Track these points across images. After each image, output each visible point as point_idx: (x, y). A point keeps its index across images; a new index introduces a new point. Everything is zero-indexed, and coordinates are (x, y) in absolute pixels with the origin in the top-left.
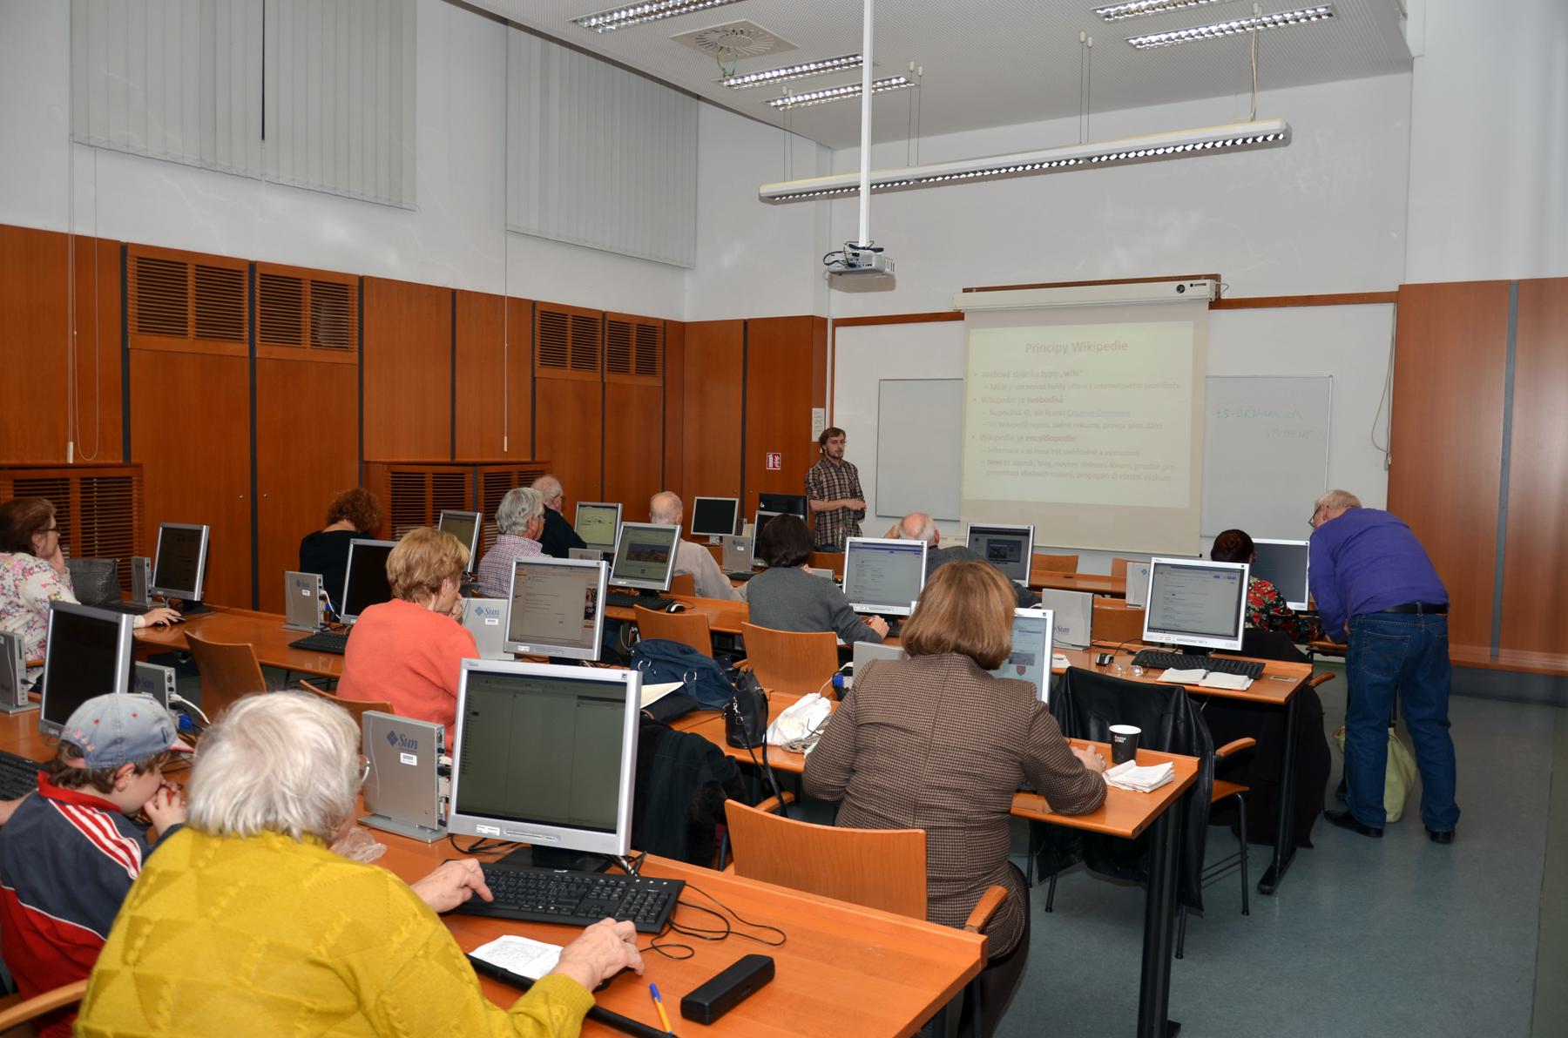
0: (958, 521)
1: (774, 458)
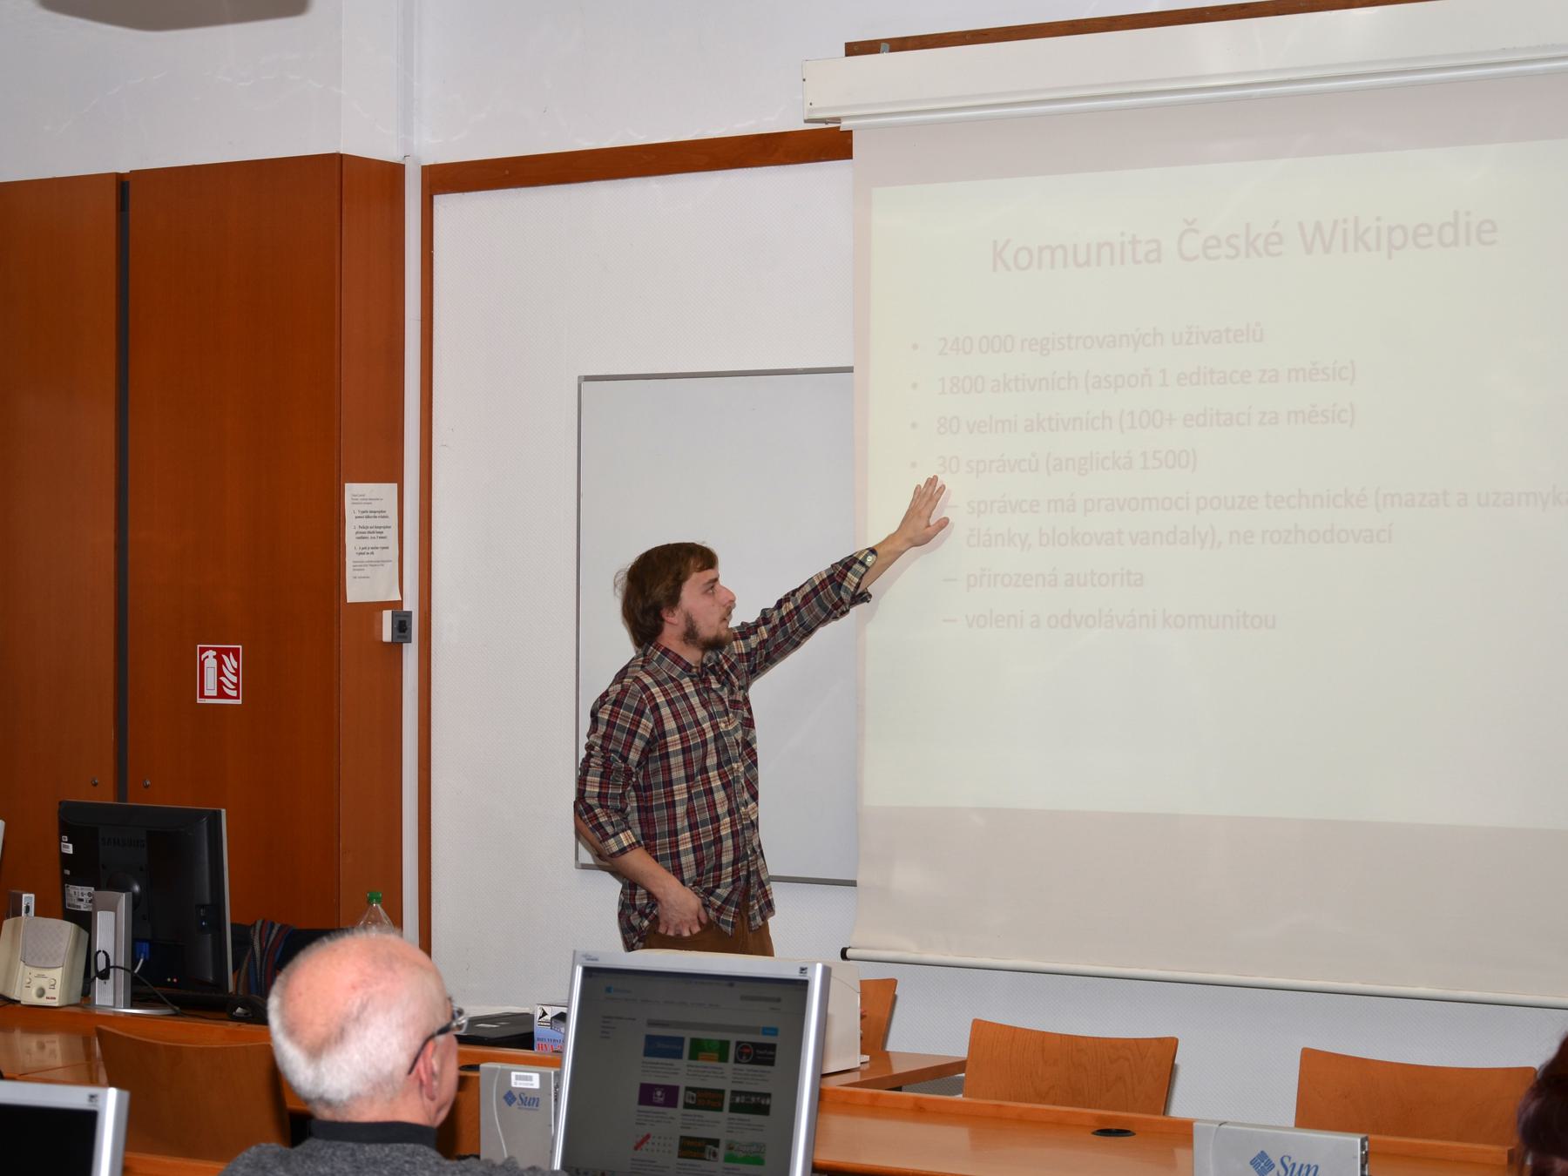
0: (853, 884)
1: (221, 663)
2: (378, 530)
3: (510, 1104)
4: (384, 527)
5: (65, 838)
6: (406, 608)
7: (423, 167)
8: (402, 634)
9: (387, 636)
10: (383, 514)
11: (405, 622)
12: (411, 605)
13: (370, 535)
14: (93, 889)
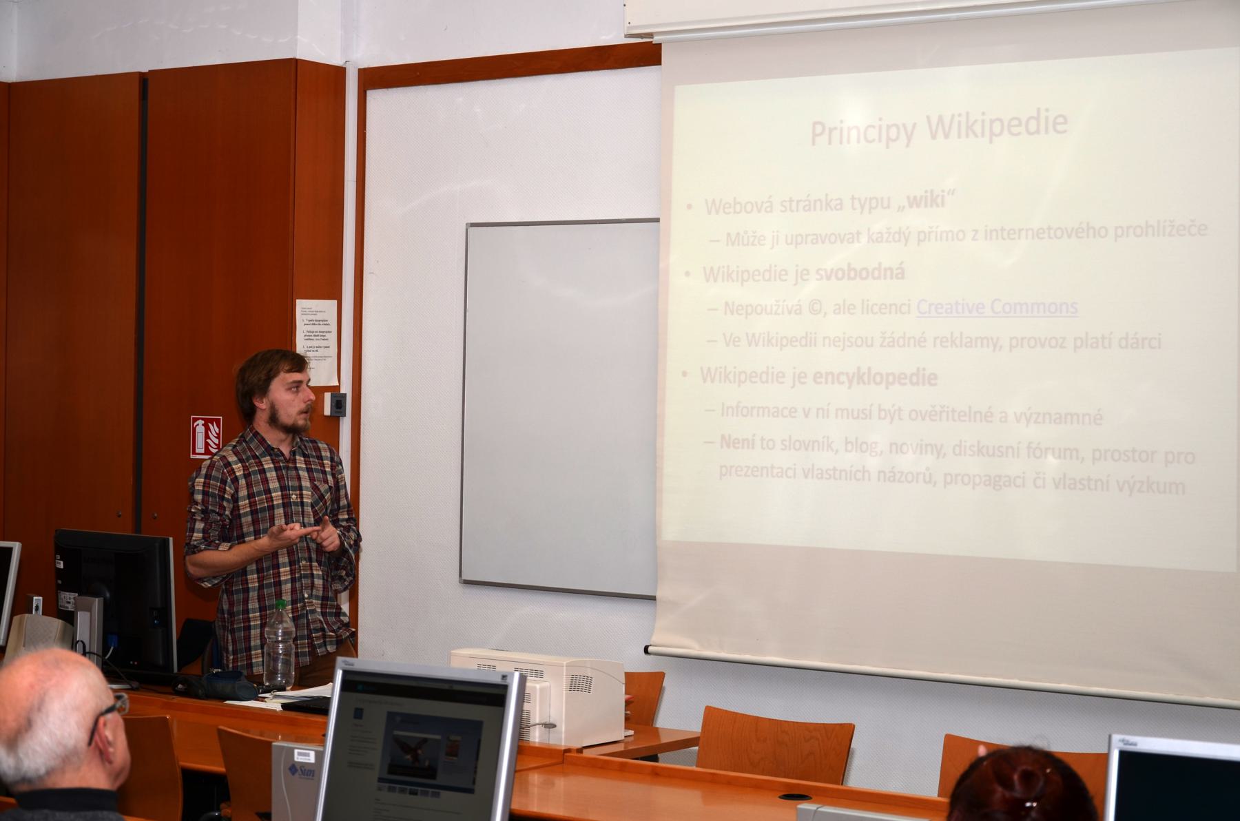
0: (653, 598)
1: (207, 429)
2: (321, 334)
3: (293, 774)
4: (327, 332)
5: (58, 557)
6: (342, 391)
7: (359, 69)
8: (339, 410)
9: (327, 411)
10: (325, 323)
11: (340, 401)
12: (346, 389)
13: (315, 338)
14: (77, 594)
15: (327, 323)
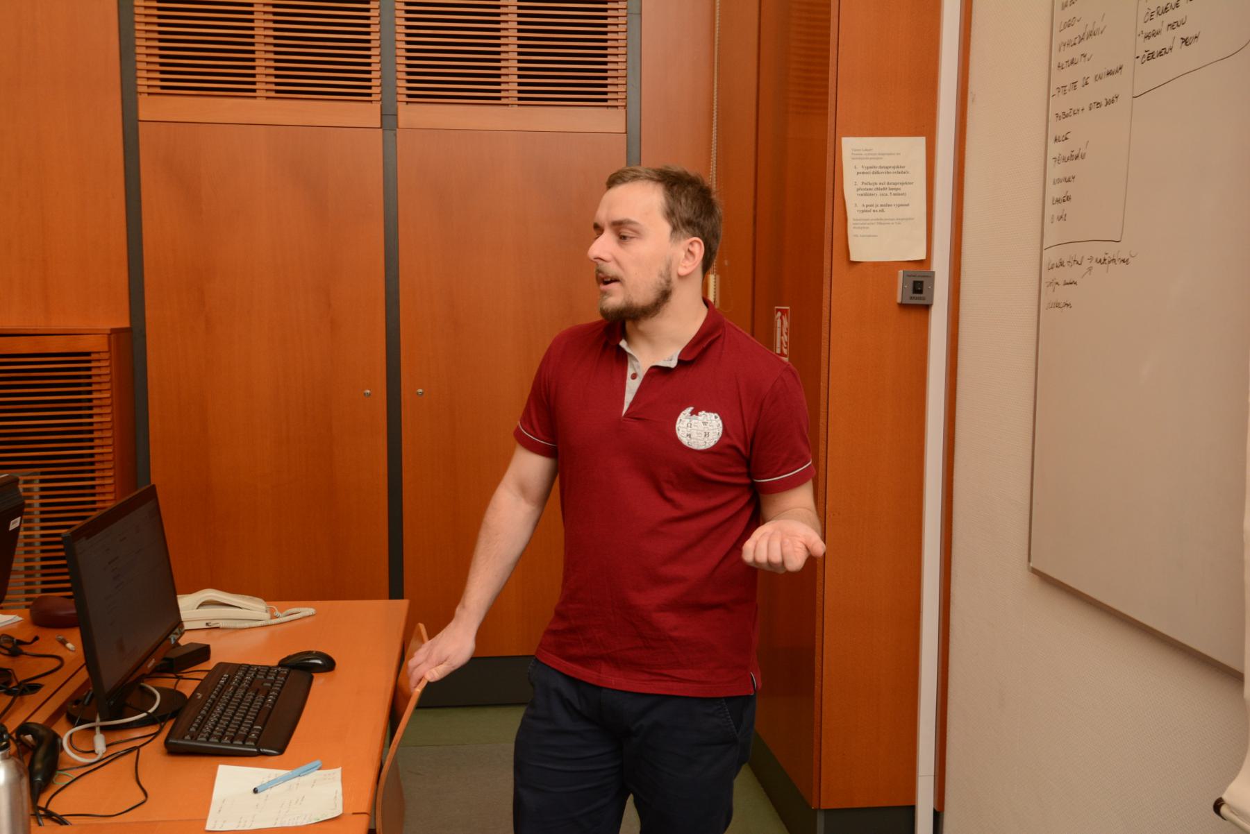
4: (903, 184)
10: (900, 170)
15: (904, 170)
